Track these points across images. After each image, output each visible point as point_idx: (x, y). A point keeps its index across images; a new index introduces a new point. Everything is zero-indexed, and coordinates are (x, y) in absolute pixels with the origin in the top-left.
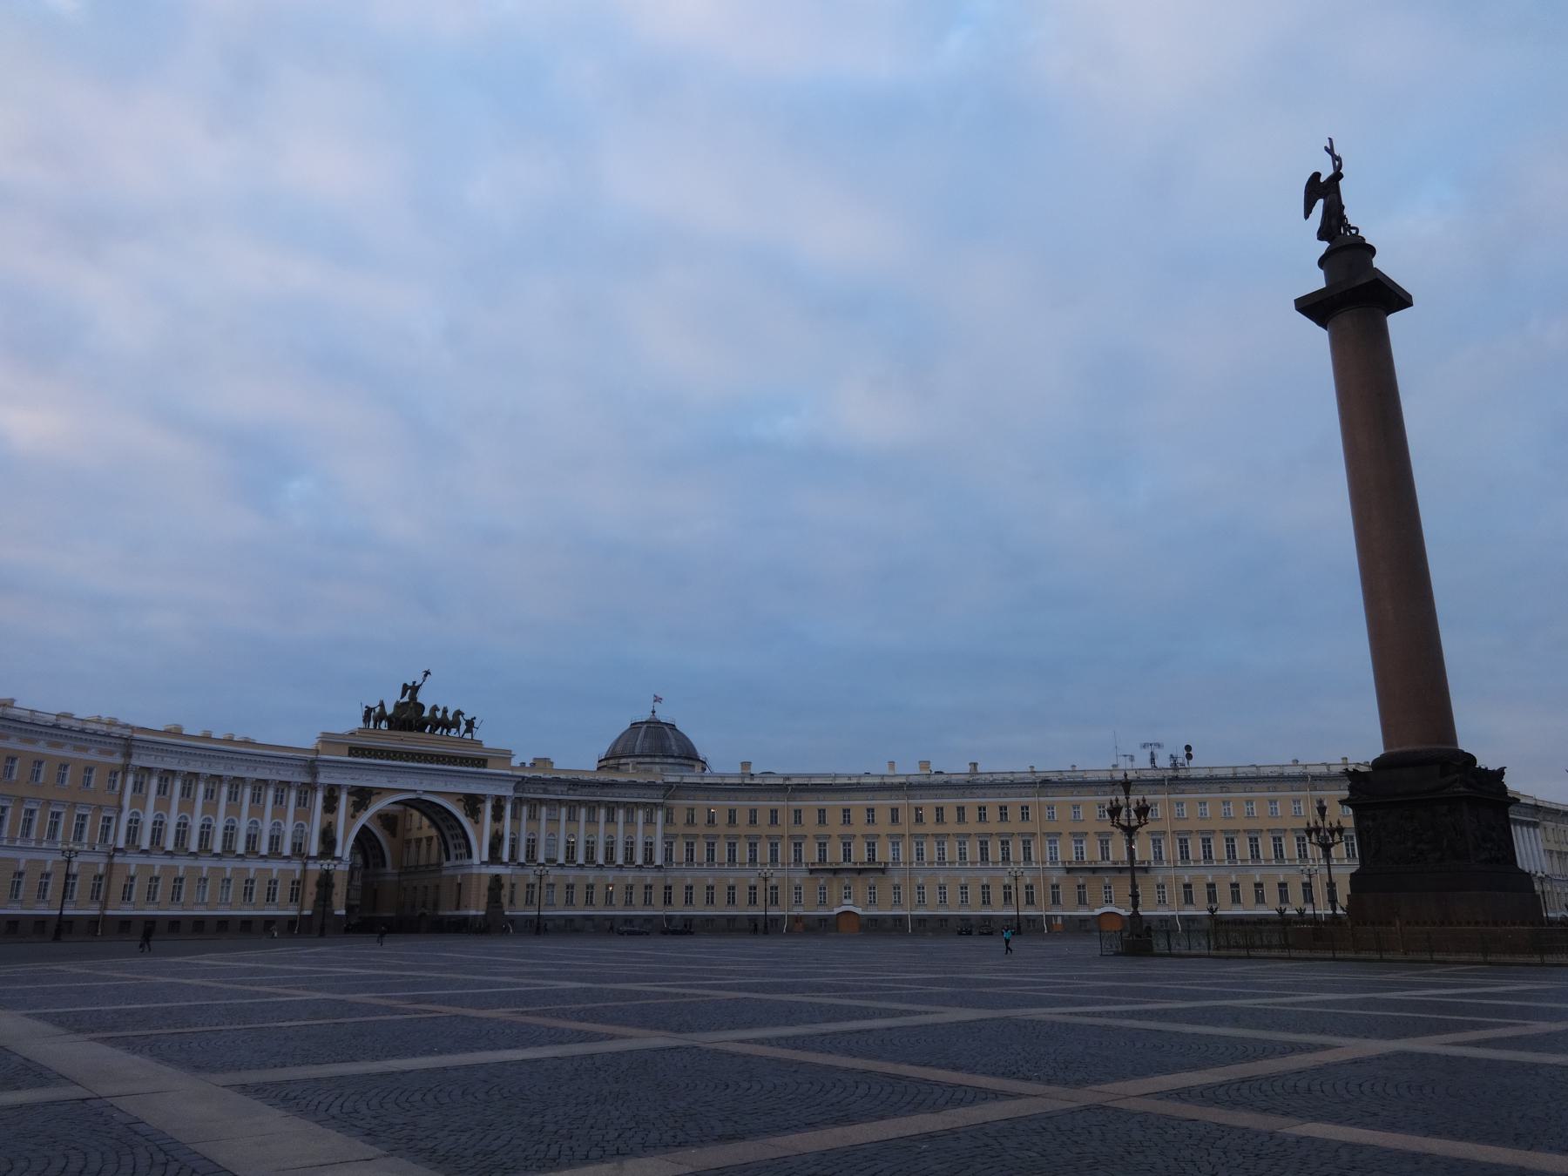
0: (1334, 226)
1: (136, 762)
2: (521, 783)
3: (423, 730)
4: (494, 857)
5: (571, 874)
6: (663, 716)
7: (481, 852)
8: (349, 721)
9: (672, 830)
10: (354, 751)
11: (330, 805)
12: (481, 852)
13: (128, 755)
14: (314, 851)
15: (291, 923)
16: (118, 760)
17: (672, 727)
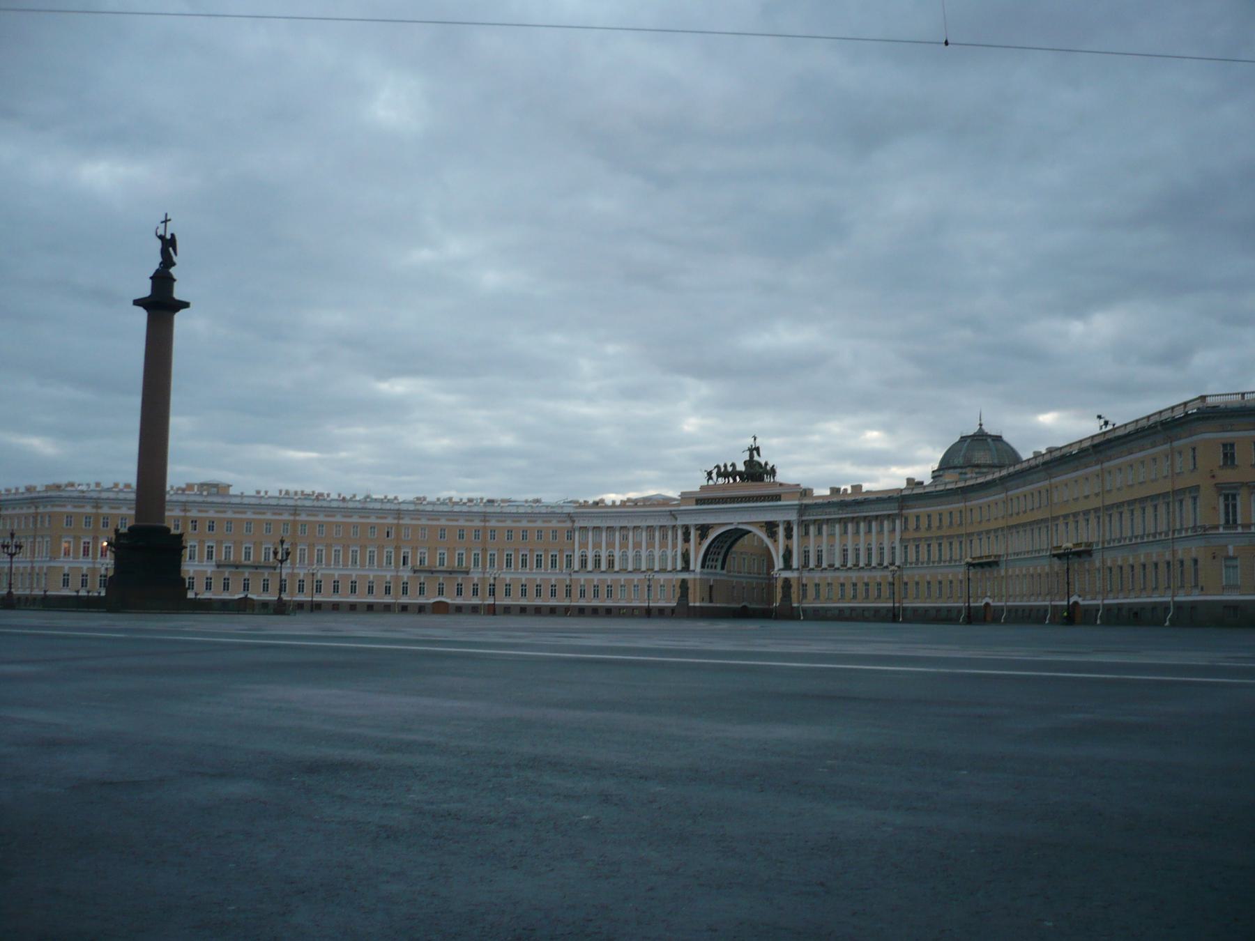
0: (167, 262)
1: (576, 525)
2: (803, 509)
3: (762, 480)
4: (788, 566)
5: (842, 575)
6: (990, 429)
7: (779, 563)
8: (696, 482)
9: (906, 536)
10: (699, 501)
11: (686, 540)
12: (779, 563)
13: (573, 522)
14: (679, 568)
15: (673, 610)
16: (569, 524)
17: (998, 439)
